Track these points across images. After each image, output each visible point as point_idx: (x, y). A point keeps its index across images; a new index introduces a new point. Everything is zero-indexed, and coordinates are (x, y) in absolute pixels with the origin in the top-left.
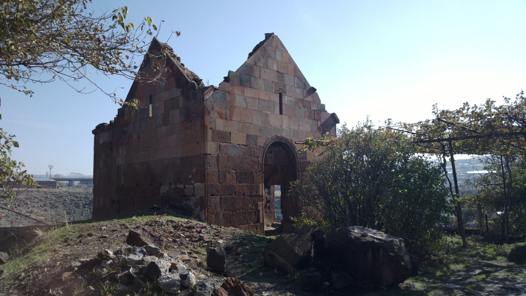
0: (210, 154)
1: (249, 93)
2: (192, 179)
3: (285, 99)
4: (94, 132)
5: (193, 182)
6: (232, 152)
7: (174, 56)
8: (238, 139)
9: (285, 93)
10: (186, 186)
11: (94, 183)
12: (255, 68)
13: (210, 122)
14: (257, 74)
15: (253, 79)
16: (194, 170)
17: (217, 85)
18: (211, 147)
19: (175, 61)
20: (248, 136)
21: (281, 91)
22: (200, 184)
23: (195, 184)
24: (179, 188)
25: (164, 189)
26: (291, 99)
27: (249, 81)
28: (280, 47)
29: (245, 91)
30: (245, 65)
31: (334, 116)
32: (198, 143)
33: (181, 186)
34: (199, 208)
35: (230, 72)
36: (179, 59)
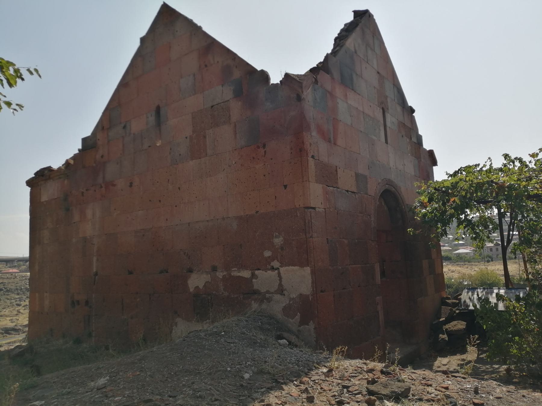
0: (314, 208)
2: (272, 258)
3: (389, 118)
4: (29, 183)
5: (276, 264)
9: (388, 109)
10: (257, 272)
11: (31, 268)
13: (311, 144)
15: (354, 76)
16: (278, 241)
18: (316, 194)
20: (357, 175)
22: (296, 268)
23: (282, 270)
27: (352, 80)
29: (348, 94)
31: (431, 153)
32: (285, 187)
33: (246, 274)
34: (298, 317)
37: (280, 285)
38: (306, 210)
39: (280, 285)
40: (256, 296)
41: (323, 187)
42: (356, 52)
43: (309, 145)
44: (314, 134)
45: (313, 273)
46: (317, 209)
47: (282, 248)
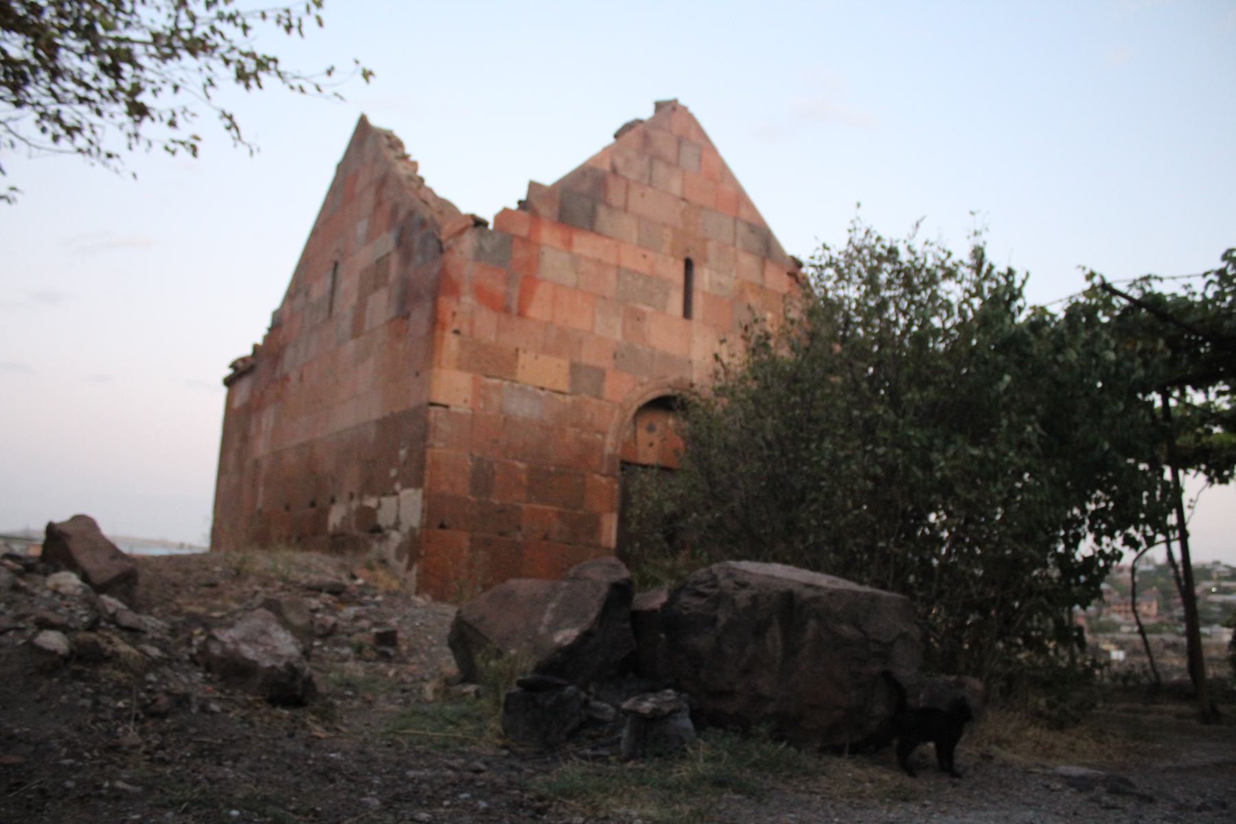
0: (447, 406)
1: (585, 245)
2: (395, 479)
3: (704, 278)
6: (522, 408)
7: (405, 157)
8: (542, 371)
9: (706, 260)
10: (384, 500)
12: (611, 181)
14: (616, 197)
15: (602, 211)
16: (403, 452)
17: (488, 214)
18: (453, 386)
19: (401, 168)
20: (575, 368)
21: (692, 256)
24: (369, 508)
25: (336, 517)
26: (724, 279)
28: (693, 135)
30: (584, 173)
33: (371, 502)
34: (405, 561)
35: (533, 186)
36: (415, 164)
37: (398, 517)
38: (433, 409)
39: (398, 517)
40: (378, 535)
41: (474, 379)
42: (614, 171)
43: (449, 314)
44: (468, 300)
45: (425, 496)
46: (453, 409)
47: (405, 464)
